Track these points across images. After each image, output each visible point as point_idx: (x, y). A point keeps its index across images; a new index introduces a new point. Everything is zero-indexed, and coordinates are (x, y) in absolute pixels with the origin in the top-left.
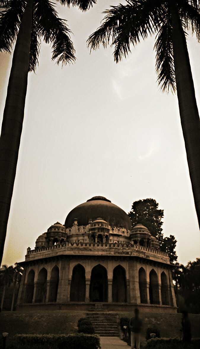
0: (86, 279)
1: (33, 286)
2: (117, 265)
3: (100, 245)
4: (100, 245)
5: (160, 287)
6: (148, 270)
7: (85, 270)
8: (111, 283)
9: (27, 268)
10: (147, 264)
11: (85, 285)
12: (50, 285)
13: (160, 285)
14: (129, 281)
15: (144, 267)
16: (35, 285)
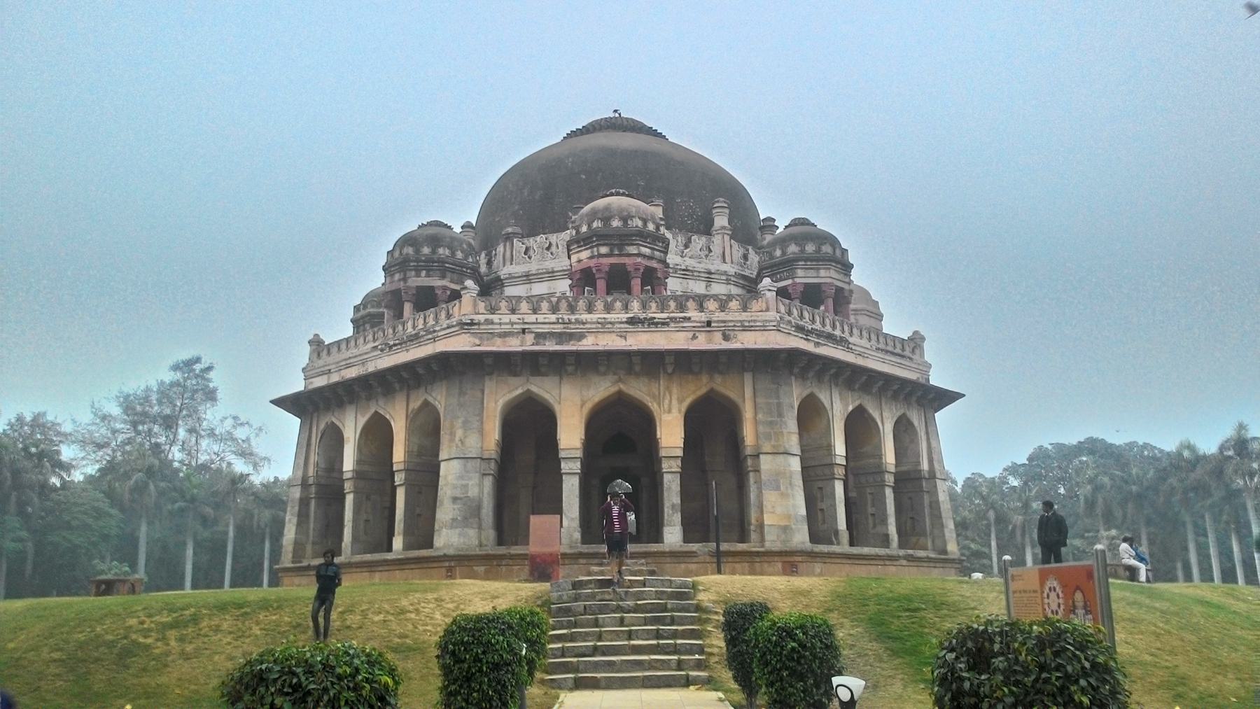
0: (562, 454)
1: (342, 488)
2: (704, 390)
4: (618, 304)
5: (890, 479)
6: (838, 407)
7: (558, 416)
8: (676, 466)
9: (315, 415)
10: (837, 385)
11: (558, 477)
12: (408, 484)
13: (892, 469)
14: (757, 456)
15: (823, 397)
16: (348, 486)
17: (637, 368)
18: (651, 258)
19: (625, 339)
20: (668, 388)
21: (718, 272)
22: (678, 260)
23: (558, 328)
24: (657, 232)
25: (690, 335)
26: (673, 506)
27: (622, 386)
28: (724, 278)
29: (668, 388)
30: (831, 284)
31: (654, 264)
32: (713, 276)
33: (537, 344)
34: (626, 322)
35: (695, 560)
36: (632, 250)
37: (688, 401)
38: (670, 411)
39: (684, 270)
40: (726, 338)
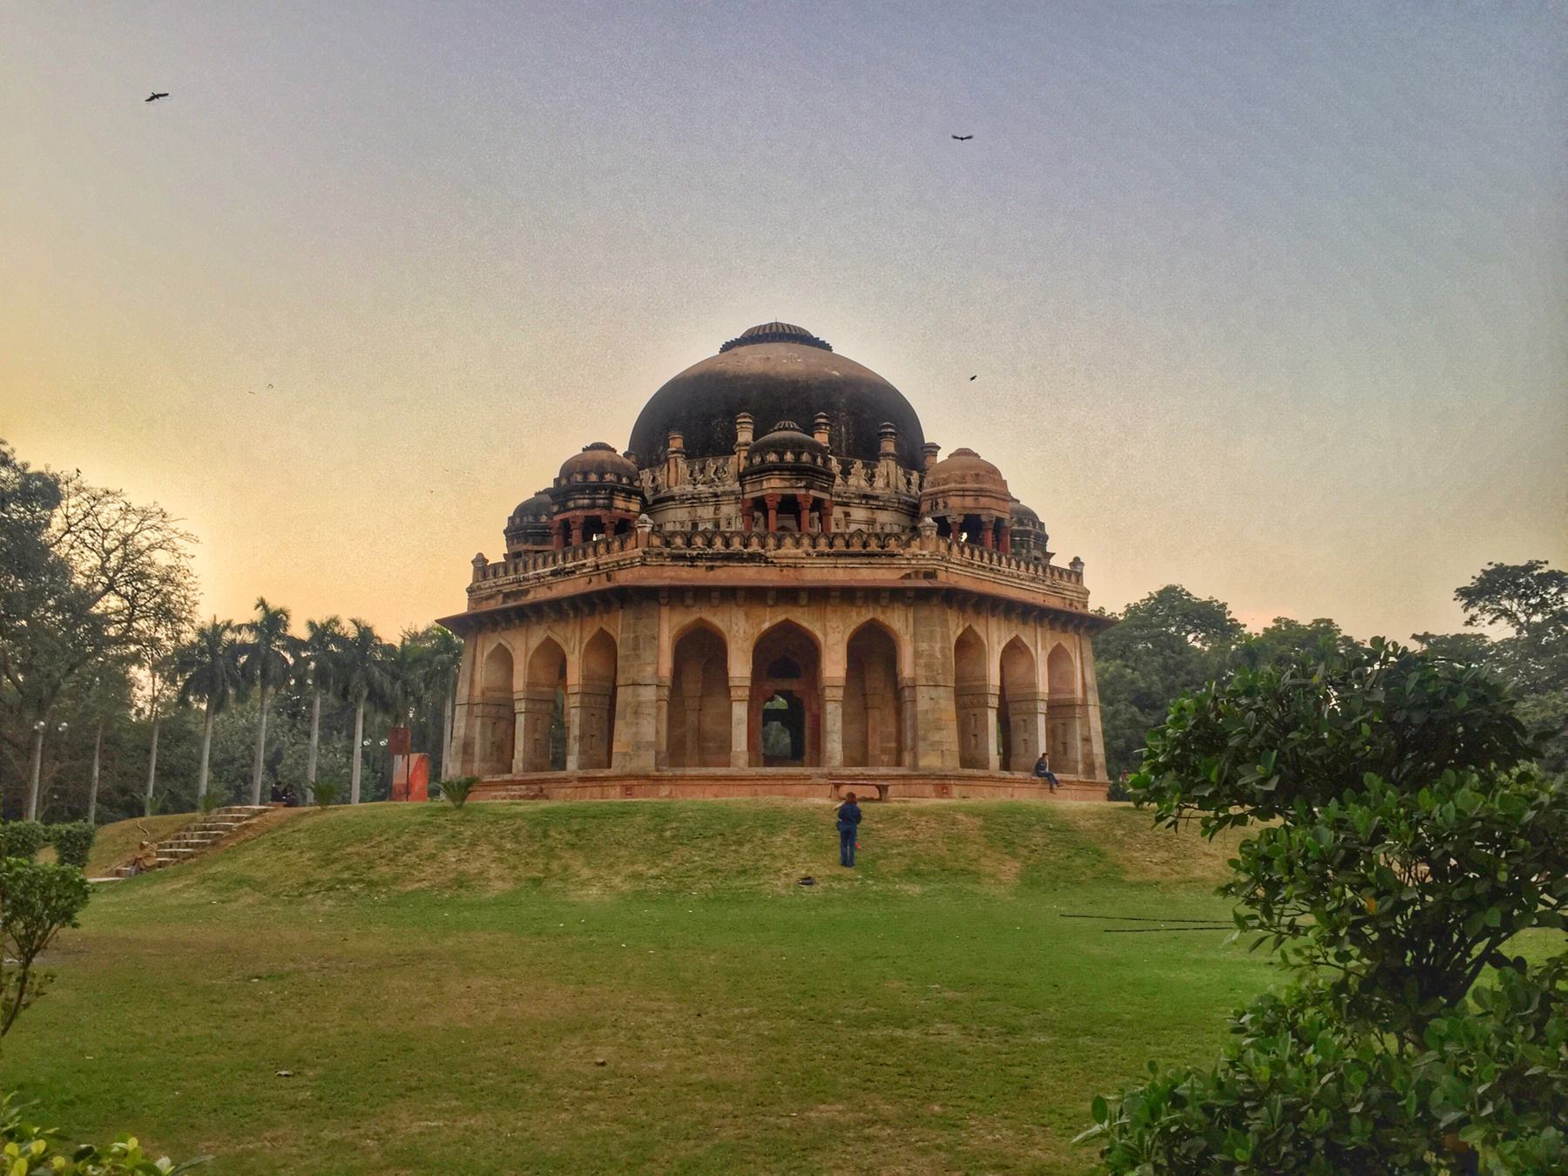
3: (788, 541)
17: (553, 615)
18: (593, 506)
19: (550, 588)
20: (574, 633)
21: (724, 493)
22: (689, 488)
23: (514, 588)
24: (601, 481)
25: (587, 579)
26: (575, 737)
27: (549, 633)
28: (733, 497)
29: (574, 633)
30: (771, 495)
31: (597, 512)
32: (720, 499)
33: (504, 602)
34: (551, 575)
35: (570, 785)
36: (571, 504)
37: (586, 641)
38: (573, 653)
39: (687, 499)
40: (609, 579)
